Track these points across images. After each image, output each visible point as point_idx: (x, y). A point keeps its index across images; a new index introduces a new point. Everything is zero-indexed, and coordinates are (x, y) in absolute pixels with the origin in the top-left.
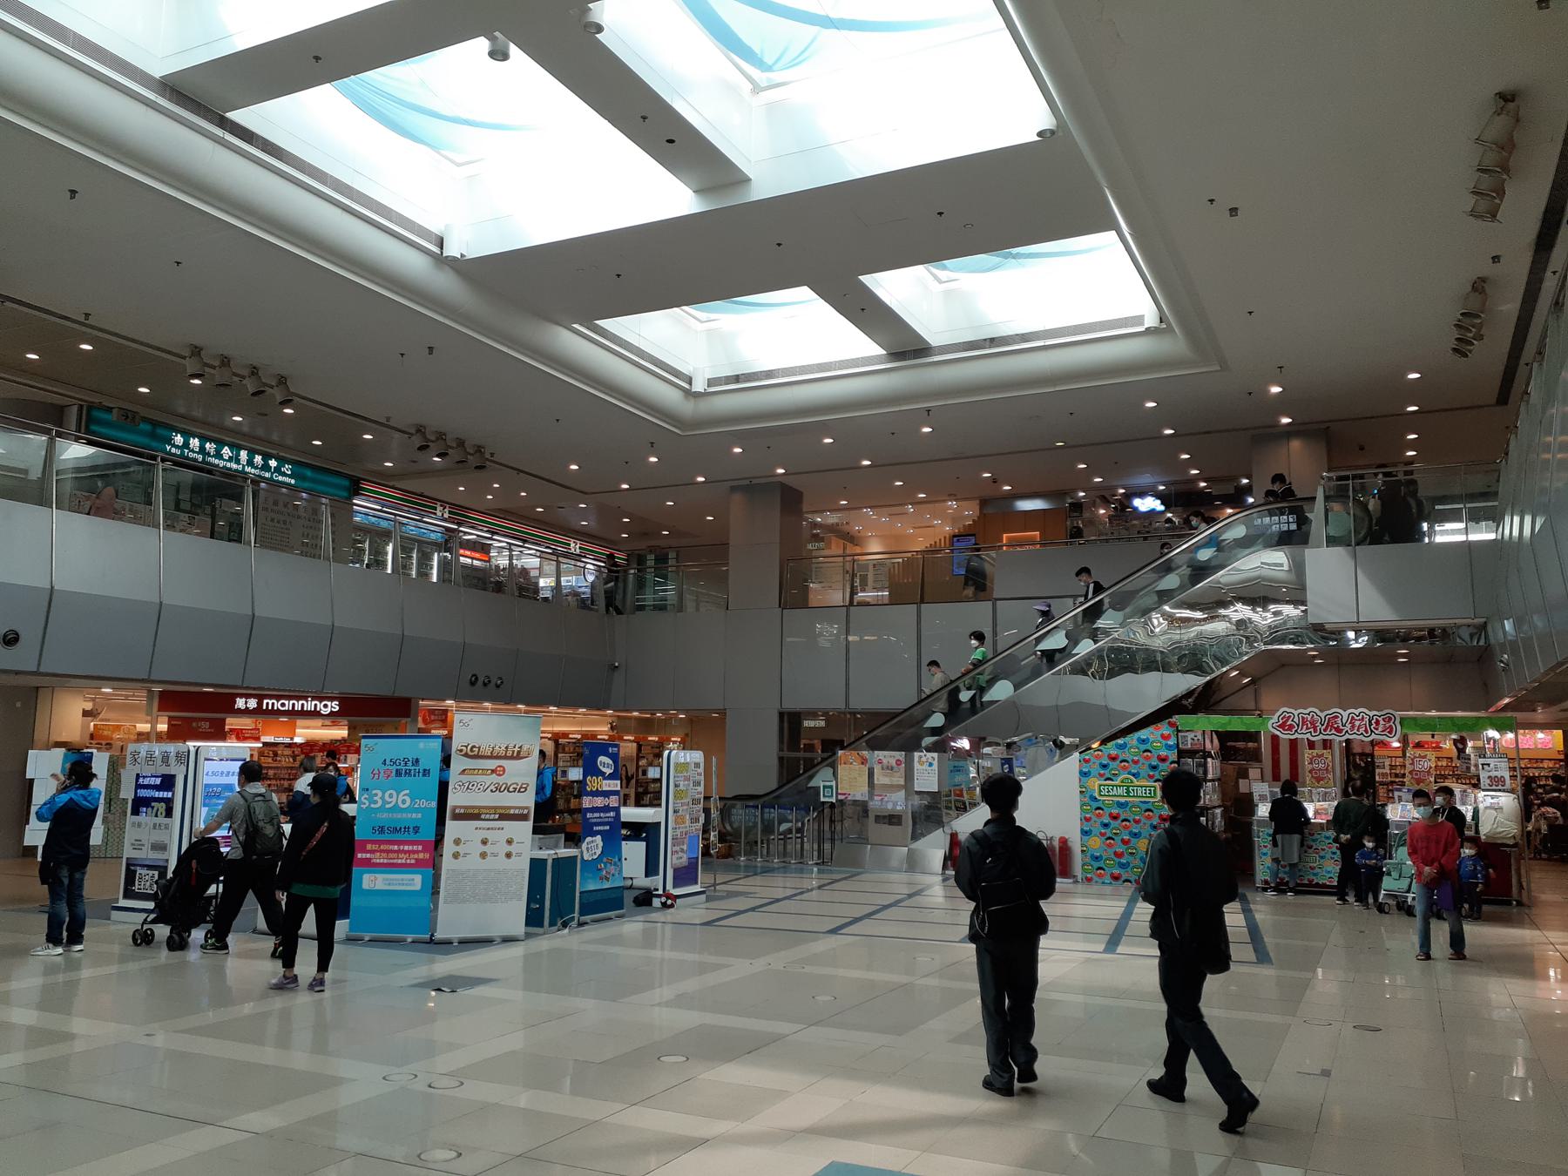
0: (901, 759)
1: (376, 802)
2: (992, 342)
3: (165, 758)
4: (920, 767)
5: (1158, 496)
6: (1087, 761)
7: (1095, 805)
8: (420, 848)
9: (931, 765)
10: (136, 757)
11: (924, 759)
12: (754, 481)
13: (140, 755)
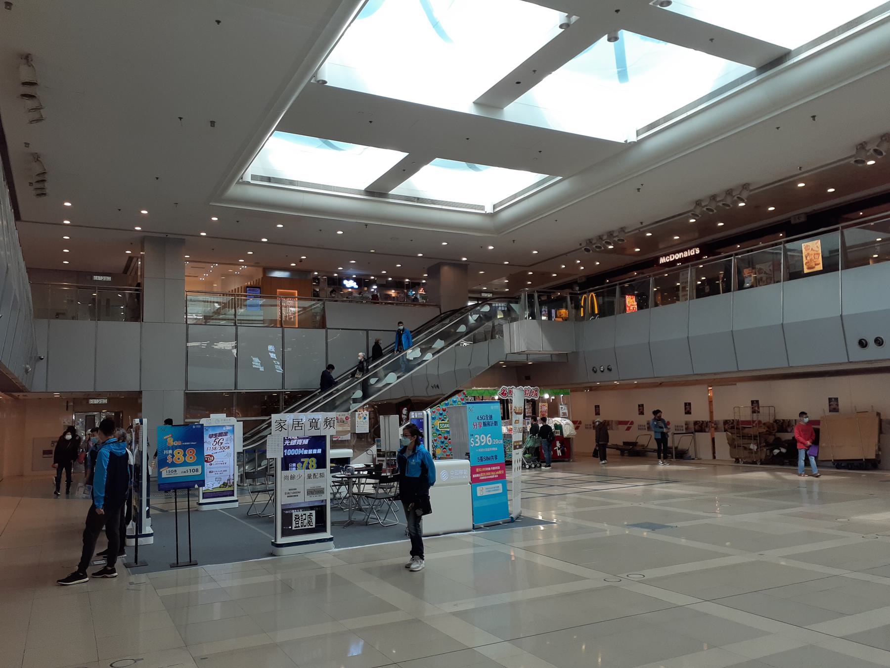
0: (348, 416)
1: (477, 443)
2: (418, 200)
3: (314, 424)
4: (359, 420)
5: (355, 280)
6: (434, 412)
7: (438, 433)
8: (499, 468)
9: (365, 418)
10: (282, 424)
11: (361, 415)
12: (169, 236)
13: (286, 423)
